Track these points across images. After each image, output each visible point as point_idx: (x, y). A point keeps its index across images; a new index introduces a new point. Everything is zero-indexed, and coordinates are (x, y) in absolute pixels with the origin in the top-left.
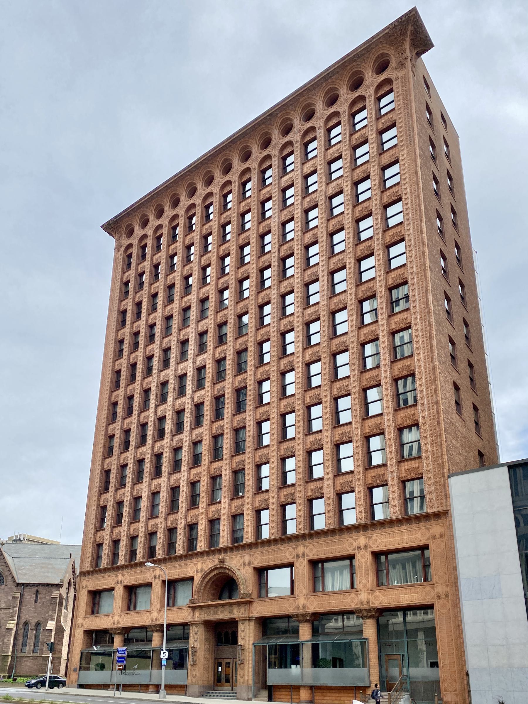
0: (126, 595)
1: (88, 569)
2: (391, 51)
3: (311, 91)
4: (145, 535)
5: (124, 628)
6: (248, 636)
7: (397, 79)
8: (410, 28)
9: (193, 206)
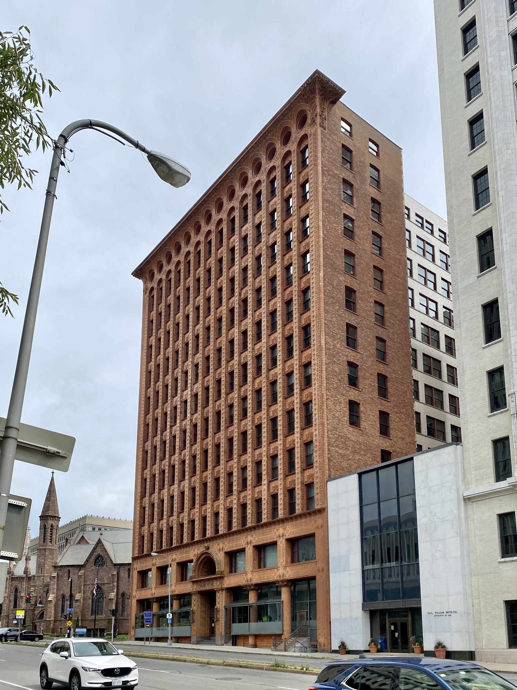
0: (228, 560)
1: (137, 555)
2: (307, 108)
3: (255, 148)
4: (284, 492)
5: (157, 598)
6: (222, 601)
7: (311, 135)
8: (317, 86)
9: (289, 153)
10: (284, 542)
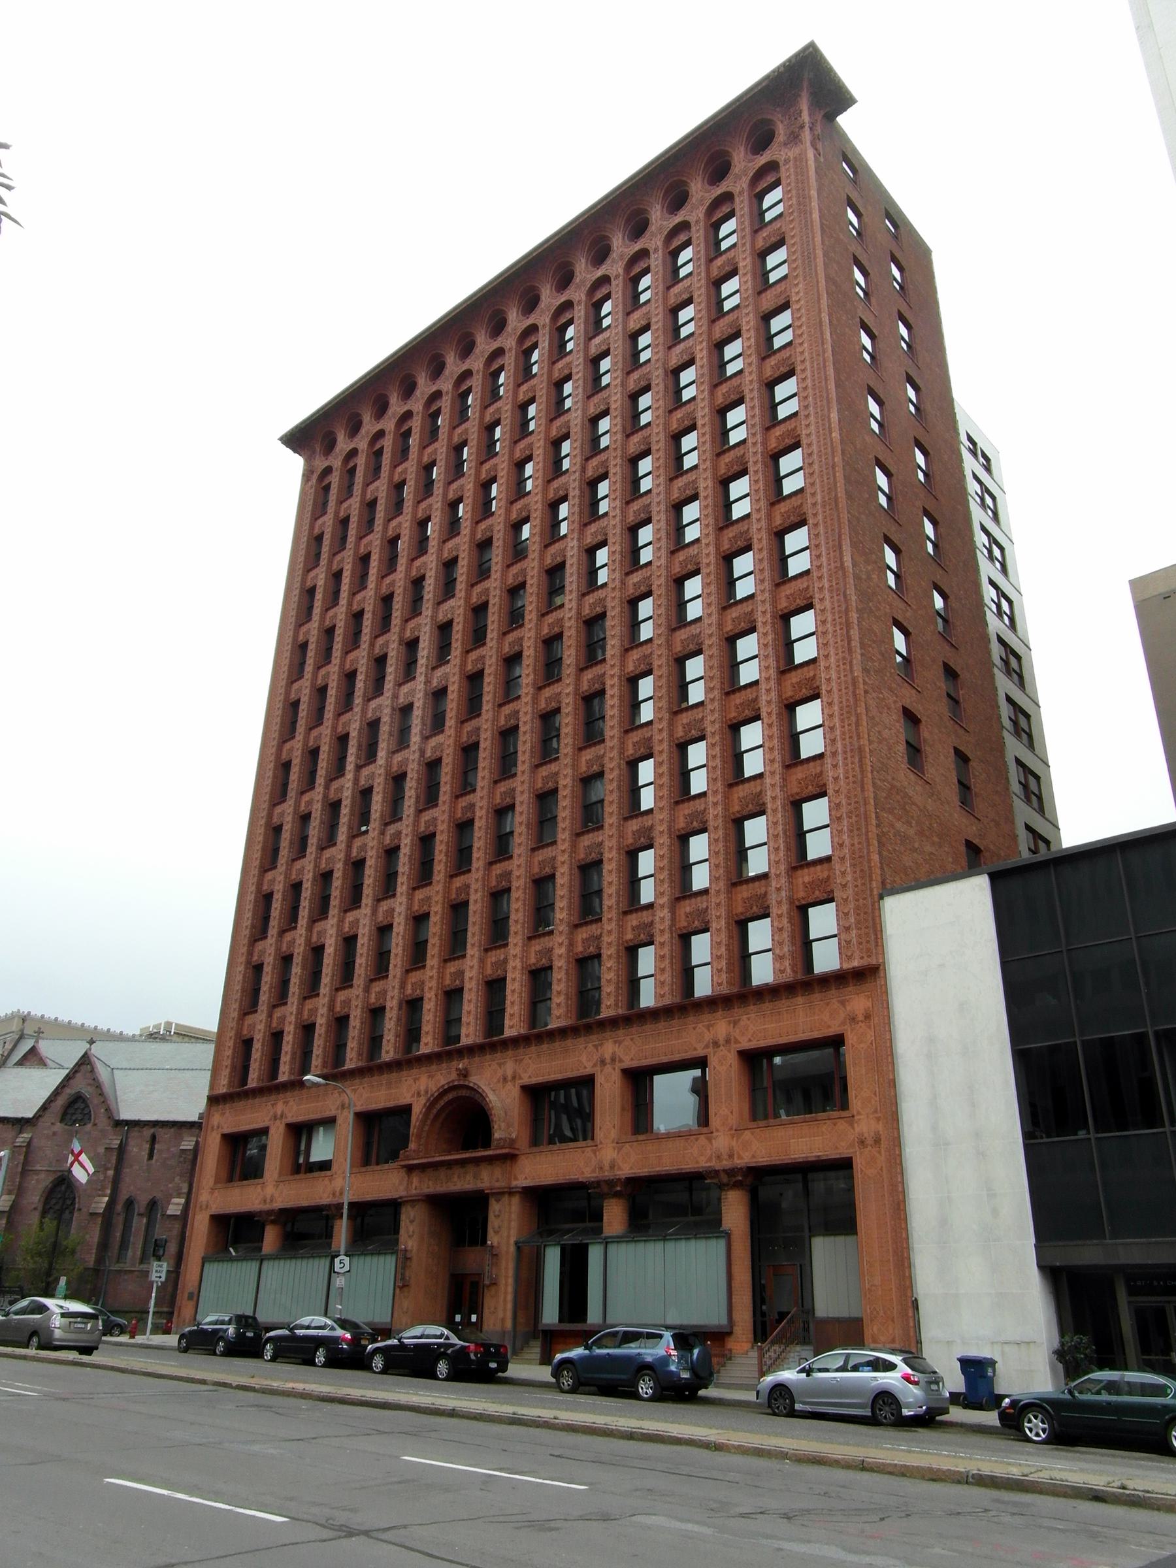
7: (787, 161)
10: (732, 1059)
